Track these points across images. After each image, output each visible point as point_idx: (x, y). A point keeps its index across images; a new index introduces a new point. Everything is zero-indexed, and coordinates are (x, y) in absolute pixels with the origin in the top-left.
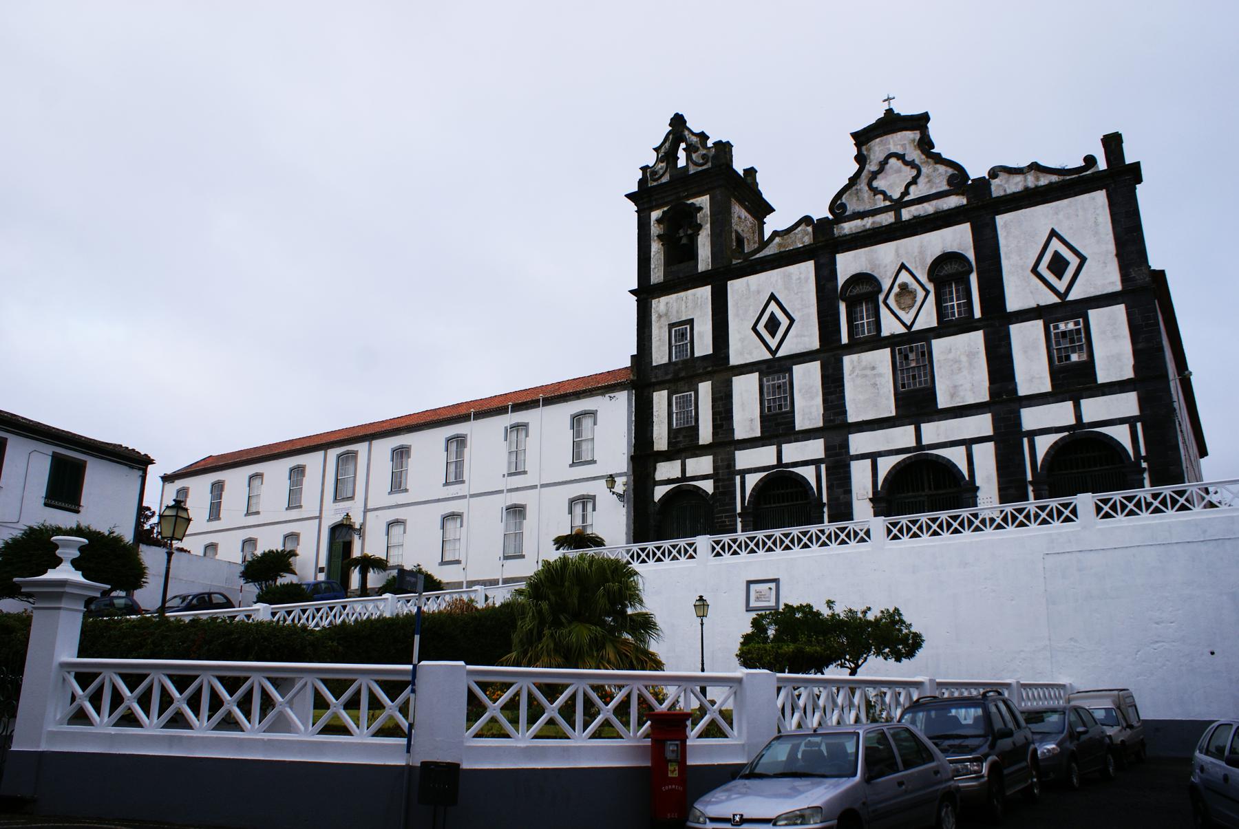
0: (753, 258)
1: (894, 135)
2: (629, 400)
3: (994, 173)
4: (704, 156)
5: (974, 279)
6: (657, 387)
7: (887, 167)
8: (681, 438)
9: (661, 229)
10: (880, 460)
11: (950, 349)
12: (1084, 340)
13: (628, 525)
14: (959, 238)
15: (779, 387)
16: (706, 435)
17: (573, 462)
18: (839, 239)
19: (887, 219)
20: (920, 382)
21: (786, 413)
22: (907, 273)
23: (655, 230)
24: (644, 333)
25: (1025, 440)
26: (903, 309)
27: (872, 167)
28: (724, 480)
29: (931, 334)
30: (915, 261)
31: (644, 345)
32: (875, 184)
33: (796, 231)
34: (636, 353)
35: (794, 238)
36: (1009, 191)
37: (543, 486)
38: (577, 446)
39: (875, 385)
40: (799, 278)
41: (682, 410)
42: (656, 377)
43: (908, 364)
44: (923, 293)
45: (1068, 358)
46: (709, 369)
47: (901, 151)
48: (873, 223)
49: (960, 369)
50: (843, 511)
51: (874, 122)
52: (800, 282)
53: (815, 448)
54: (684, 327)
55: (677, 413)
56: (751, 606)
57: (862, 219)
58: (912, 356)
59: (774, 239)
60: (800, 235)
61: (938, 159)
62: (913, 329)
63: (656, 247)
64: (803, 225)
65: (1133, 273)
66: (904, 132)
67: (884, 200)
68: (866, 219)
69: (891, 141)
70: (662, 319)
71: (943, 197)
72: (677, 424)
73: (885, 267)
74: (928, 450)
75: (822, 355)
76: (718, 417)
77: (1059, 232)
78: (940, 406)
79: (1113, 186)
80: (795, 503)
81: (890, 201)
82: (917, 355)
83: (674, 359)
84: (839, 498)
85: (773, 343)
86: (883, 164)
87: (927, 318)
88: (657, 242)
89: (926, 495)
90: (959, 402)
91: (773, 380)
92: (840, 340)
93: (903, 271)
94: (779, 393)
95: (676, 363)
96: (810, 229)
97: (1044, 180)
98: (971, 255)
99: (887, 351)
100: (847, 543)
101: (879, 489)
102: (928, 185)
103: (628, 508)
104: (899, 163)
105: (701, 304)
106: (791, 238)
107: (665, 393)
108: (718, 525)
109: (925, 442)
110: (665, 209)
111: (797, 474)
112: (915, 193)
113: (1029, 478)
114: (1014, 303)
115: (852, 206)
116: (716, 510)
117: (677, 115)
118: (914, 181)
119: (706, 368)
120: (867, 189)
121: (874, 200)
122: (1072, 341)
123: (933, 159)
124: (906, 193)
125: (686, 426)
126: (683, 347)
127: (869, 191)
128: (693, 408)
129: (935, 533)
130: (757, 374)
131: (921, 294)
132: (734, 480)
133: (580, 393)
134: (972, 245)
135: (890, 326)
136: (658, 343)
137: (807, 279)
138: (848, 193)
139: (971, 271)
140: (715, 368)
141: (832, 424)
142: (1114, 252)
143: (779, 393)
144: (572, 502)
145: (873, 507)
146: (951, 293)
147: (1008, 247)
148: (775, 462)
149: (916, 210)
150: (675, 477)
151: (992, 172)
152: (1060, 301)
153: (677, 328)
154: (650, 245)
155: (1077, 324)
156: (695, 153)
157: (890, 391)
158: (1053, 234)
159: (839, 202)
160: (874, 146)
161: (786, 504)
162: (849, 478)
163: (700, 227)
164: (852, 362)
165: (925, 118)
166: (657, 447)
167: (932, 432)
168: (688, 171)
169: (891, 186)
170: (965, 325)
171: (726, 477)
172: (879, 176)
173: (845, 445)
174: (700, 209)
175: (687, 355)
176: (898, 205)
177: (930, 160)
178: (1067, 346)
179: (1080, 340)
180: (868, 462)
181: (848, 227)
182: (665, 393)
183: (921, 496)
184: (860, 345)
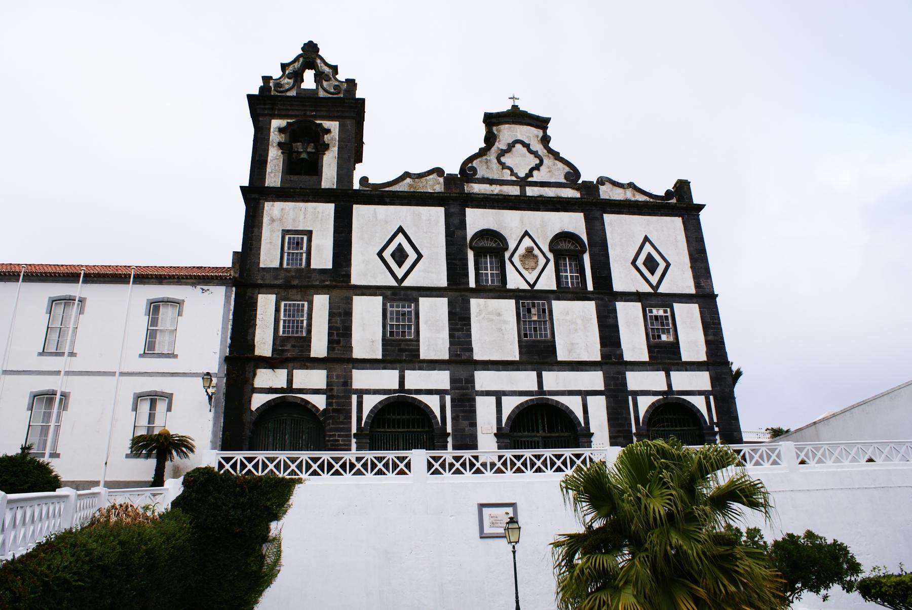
0: (384, 189)
1: (521, 127)
2: (227, 297)
3: (602, 181)
4: (336, 87)
5: (587, 258)
6: (264, 290)
7: (514, 150)
8: (289, 347)
9: (282, 138)
11: (568, 312)
12: (671, 325)
13: (215, 434)
14: (575, 222)
15: (404, 314)
16: (319, 347)
17: (144, 353)
18: (472, 195)
19: (515, 191)
20: (541, 335)
21: (411, 340)
22: (530, 240)
23: (275, 137)
24: (252, 232)
25: (630, 398)
26: (527, 269)
27: (501, 145)
28: (338, 397)
29: (551, 296)
30: (538, 232)
31: (252, 244)
32: (503, 159)
33: (428, 178)
34: (240, 250)
35: (425, 183)
36: (612, 198)
37: (122, 374)
38: (151, 335)
39: (500, 330)
40: (429, 220)
41: (291, 318)
42: (263, 279)
43: (530, 317)
44: (545, 261)
45: (659, 337)
46: (327, 283)
47: (527, 141)
48: (501, 191)
49: (576, 330)
50: (467, 440)
51: (505, 110)
52: (430, 223)
53: (441, 379)
54: (300, 236)
55: (285, 321)
56: (485, 532)
57: (491, 185)
58: (534, 311)
59: (405, 179)
60: (431, 183)
61: (556, 155)
62: (536, 288)
63: (274, 155)
64: (435, 174)
65: (702, 282)
66: (529, 127)
67: (511, 175)
68: (494, 186)
69: (518, 130)
70: (275, 224)
71: (562, 187)
72: (284, 332)
73: (511, 230)
74: (548, 395)
75: (450, 293)
76: (335, 332)
77: (651, 239)
78: (559, 359)
79: (686, 216)
80: (396, 430)
81: (516, 177)
82: (538, 311)
83: (285, 266)
84: (464, 431)
85: (400, 273)
86: (511, 146)
87: (548, 282)
88: (276, 148)
89: (540, 436)
90: (576, 358)
91: (398, 307)
92: (468, 283)
93: (527, 237)
94: (404, 320)
95: (286, 270)
96: (441, 180)
97: (641, 198)
98: (585, 238)
99: (513, 302)
100: (462, 473)
101: (503, 426)
102: (549, 174)
103: (216, 412)
104: (525, 150)
105: (322, 220)
106: (422, 182)
107: (273, 297)
108: (329, 443)
109: (546, 388)
110: (289, 121)
111: (420, 402)
112: (537, 177)
113: (634, 430)
114: (619, 285)
115: (482, 172)
116: (327, 428)
117: (311, 42)
118: (537, 167)
119: (324, 281)
120: (497, 162)
121: (502, 172)
122: (662, 324)
123: (553, 155)
124: (530, 174)
125: (295, 335)
126: (297, 256)
127: (498, 164)
128: (305, 318)
129: (519, 471)
130: (381, 298)
131: (542, 261)
132: (350, 398)
133: (165, 278)
134: (585, 231)
135: (514, 281)
136: (269, 245)
137: (437, 223)
138: (478, 160)
139: (585, 252)
140: (334, 283)
141: (459, 359)
142: (689, 265)
143: (404, 320)
144: (139, 397)
145: (497, 442)
147: (613, 240)
148: (396, 387)
149: (538, 191)
150: (280, 387)
151: (600, 180)
152: (653, 292)
153: (292, 236)
154: (268, 150)
155: (665, 312)
156: (326, 81)
157: (514, 338)
158: (646, 239)
159: (470, 165)
160: (504, 129)
161: (405, 430)
162: (474, 412)
163: (326, 147)
164: (479, 305)
165: (546, 121)
166: (258, 352)
167: (553, 380)
168: (317, 94)
170: (580, 294)
171: (341, 394)
172: (507, 155)
173: (471, 380)
174: (328, 131)
175: (301, 264)
176: (523, 182)
177: (550, 155)
178: (659, 327)
179: (668, 325)
180: (493, 399)
181: (477, 188)
182: (273, 297)
183: (536, 436)
184: (482, 291)
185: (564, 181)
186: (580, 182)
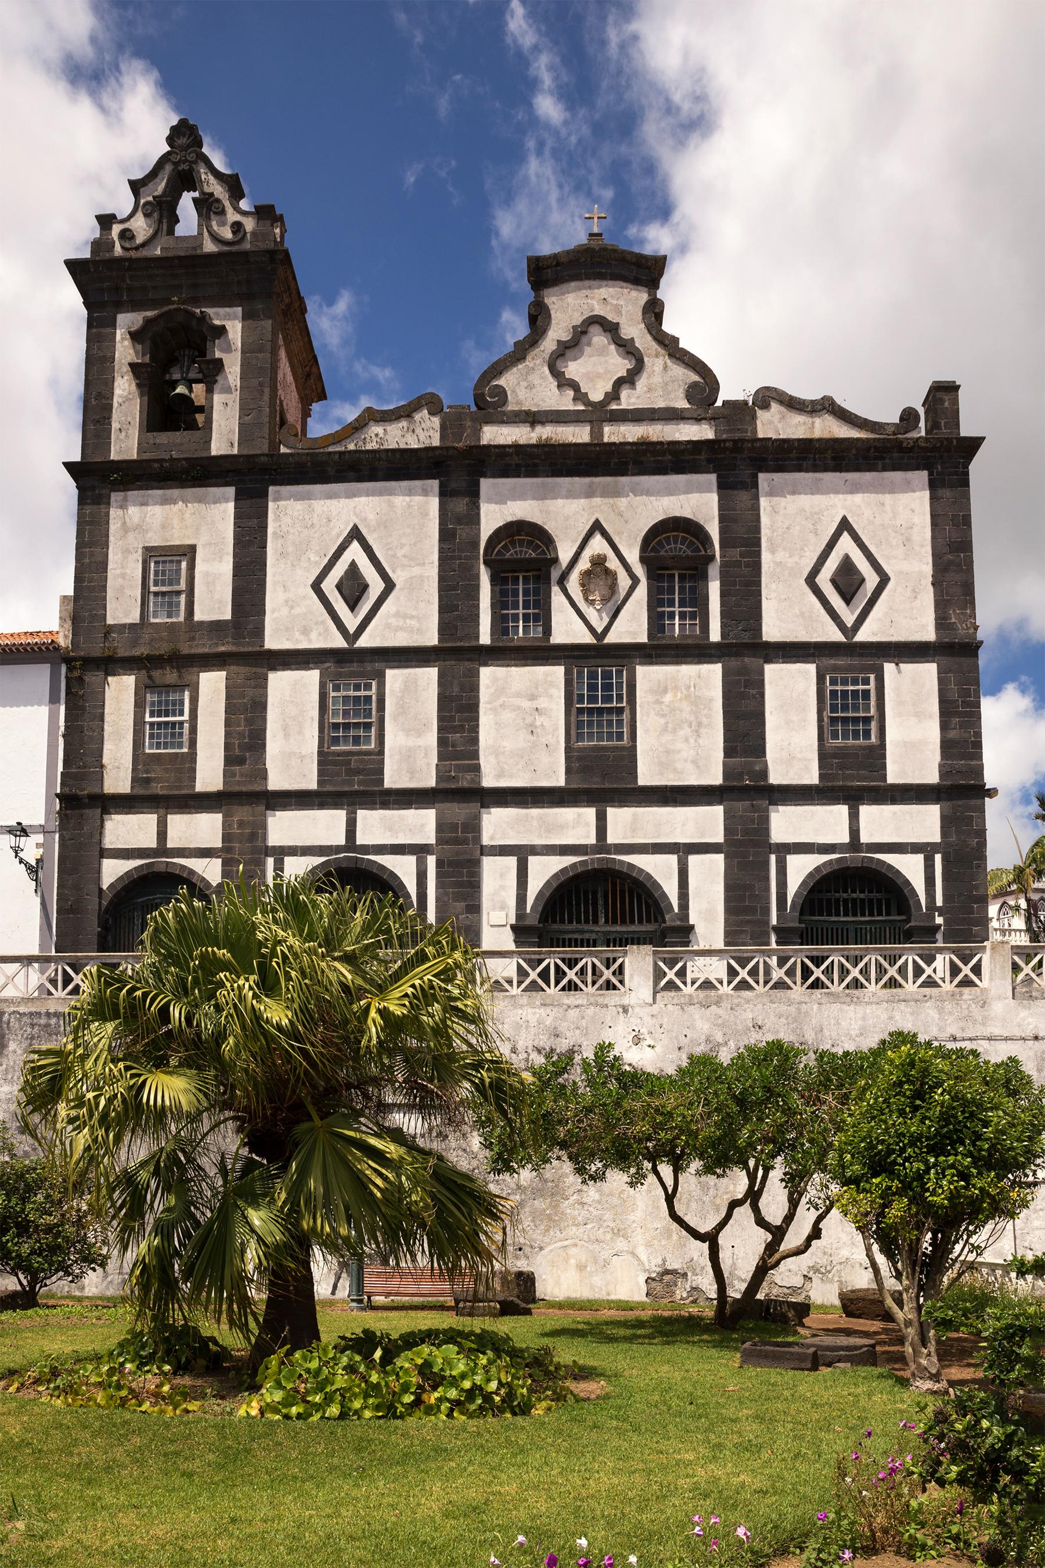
3: (766, 397)
10: (533, 860)
19: (579, 434)
21: (368, 753)
25: (773, 858)
27: (558, 332)
61: (670, 345)
62: (606, 641)
70: (131, 536)
77: (855, 526)
81: (585, 404)
85: (352, 622)
97: (844, 431)
98: (714, 530)
101: (528, 911)
109: (611, 839)
110: (150, 314)
111: (383, 868)
112: (628, 400)
113: (774, 921)
114: (773, 630)
118: (629, 380)
124: (614, 395)
146: (516, 593)
148: (341, 841)
164: (495, 680)
169: (592, 377)
173: (474, 827)
180: (512, 861)
185: (683, 404)
186: (719, 403)
